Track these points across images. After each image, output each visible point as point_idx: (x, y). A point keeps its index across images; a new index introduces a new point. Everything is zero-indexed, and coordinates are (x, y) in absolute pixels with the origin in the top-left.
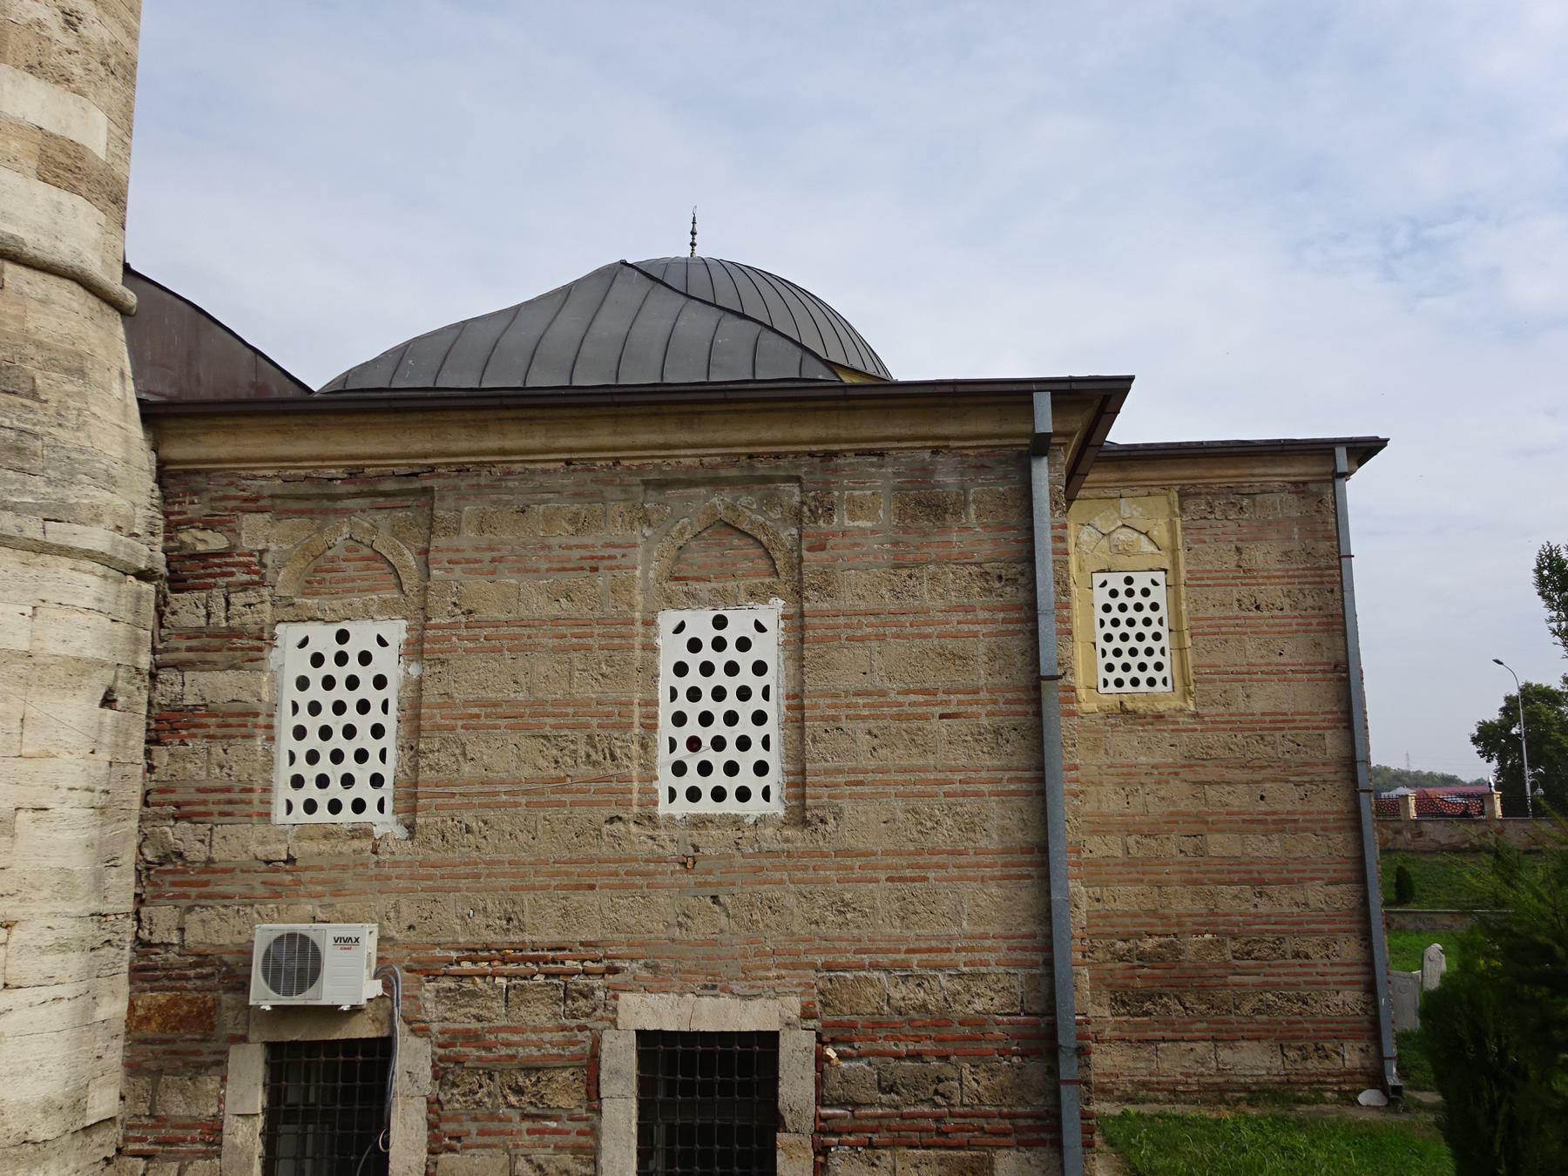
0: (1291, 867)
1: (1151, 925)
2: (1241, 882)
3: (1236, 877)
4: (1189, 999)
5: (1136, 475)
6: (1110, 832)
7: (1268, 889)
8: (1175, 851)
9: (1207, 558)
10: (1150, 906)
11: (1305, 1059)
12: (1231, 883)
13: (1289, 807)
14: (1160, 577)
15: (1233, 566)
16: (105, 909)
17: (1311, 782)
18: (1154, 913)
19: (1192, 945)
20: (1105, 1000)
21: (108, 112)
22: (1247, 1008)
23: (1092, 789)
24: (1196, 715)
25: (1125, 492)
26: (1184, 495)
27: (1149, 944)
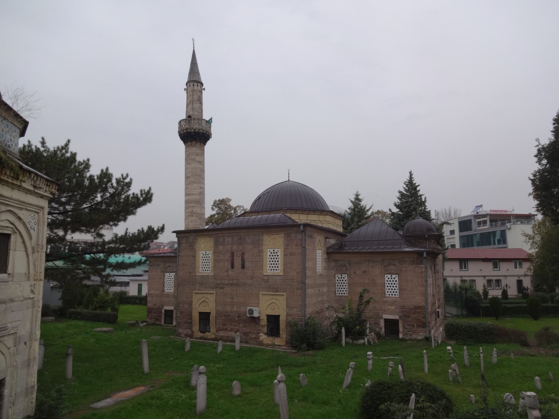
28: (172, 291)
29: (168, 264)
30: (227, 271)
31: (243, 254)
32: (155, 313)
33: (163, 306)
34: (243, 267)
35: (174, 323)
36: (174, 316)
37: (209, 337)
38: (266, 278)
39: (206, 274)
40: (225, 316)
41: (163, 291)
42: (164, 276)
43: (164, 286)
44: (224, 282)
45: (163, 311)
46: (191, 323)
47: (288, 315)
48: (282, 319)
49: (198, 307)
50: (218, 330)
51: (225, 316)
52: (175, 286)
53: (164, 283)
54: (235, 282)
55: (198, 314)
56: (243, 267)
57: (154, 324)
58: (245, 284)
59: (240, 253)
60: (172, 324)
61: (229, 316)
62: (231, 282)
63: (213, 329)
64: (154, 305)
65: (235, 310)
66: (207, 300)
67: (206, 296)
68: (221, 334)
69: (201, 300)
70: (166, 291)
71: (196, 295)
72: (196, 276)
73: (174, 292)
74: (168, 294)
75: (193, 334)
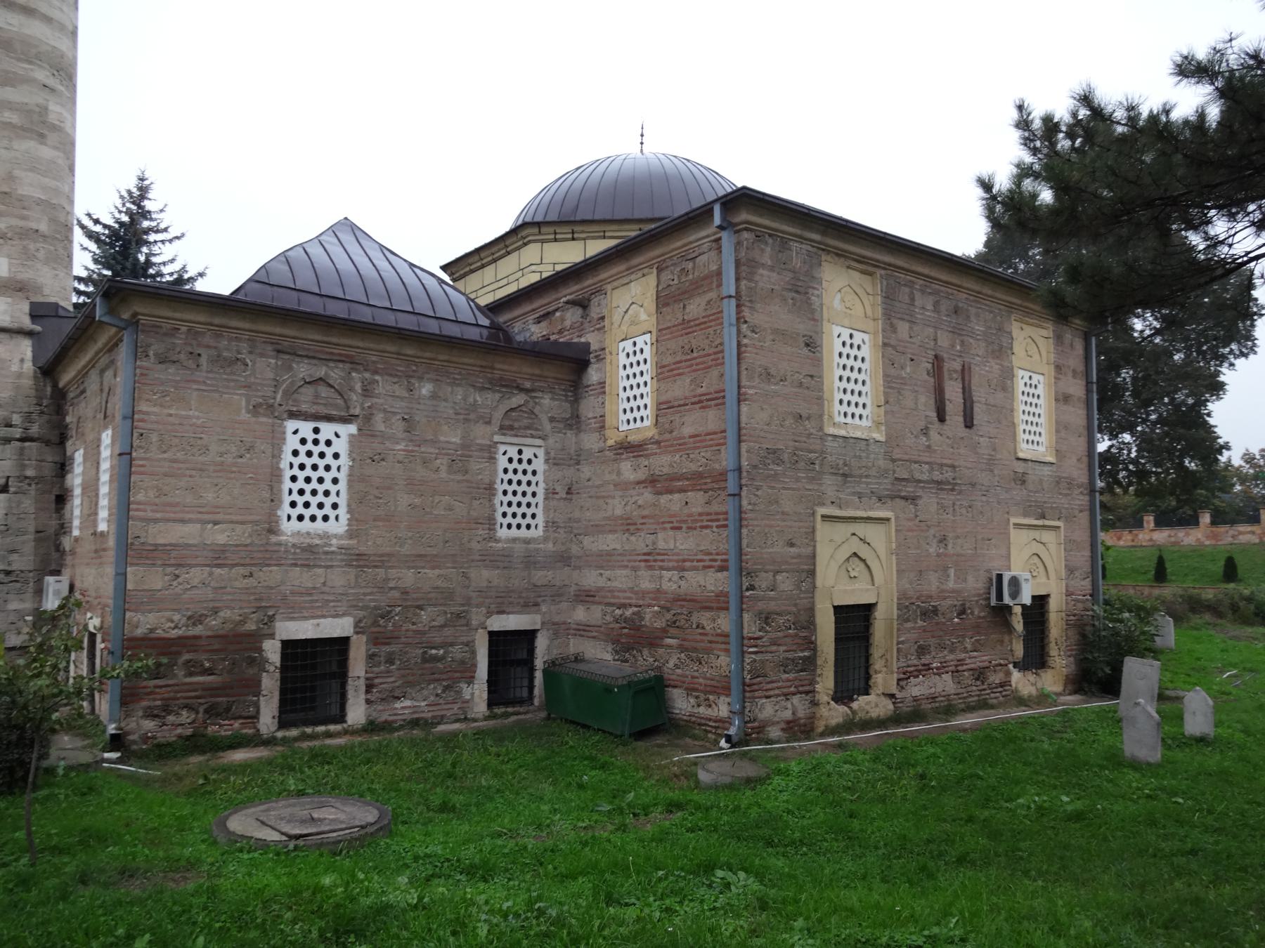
0: (699, 557)
1: (630, 598)
2: (673, 569)
3: (671, 564)
4: (645, 652)
5: (635, 261)
6: (615, 531)
7: (686, 574)
8: (643, 545)
9: (668, 318)
10: (630, 585)
11: (699, 706)
12: (668, 569)
13: (700, 510)
14: (647, 337)
15: (680, 321)
16: (9, 569)
17: (712, 489)
18: (631, 590)
19: (648, 614)
20: (610, 649)
21: (9, 256)
22: (671, 665)
23: (610, 501)
24: (658, 443)
25: (633, 277)
26: (660, 270)
27: (629, 612)
28: (338, 526)
29: (303, 370)
30: (925, 432)
31: (965, 373)
32: (193, 668)
33: (272, 619)
34: (969, 424)
35: (357, 713)
36: (358, 668)
37: (874, 713)
38: (1020, 468)
39: (858, 434)
40: (924, 614)
41: (273, 530)
42: (277, 440)
43: (275, 501)
44: (917, 476)
45: (272, 651)
46: (810, 664)
47: (1069, 594)
48: (1053, 605)
49: (838, 585)
50: (905, 677)
51: (924, 614)
52: (358, 501)
53: (276, 475)
54: (949, 475)
55: (832, 610)
56: (969, 424)
57: (196, 743)
58: (973, 485)
59: (957, 366)
60: (341, 718)
61: (935, 611)
62: (937, 476)
63: (883, 679)
64: (196, 620)
65: (951, 584)
66: (864, 552)
67: (860, 529)
68: (918, 688)
69: (845, 552)
70: (290, 528)
71: (827, 526)
72: (824, 437)
73: (351, 534)
74: (310, 549)
75: (812, 717)
